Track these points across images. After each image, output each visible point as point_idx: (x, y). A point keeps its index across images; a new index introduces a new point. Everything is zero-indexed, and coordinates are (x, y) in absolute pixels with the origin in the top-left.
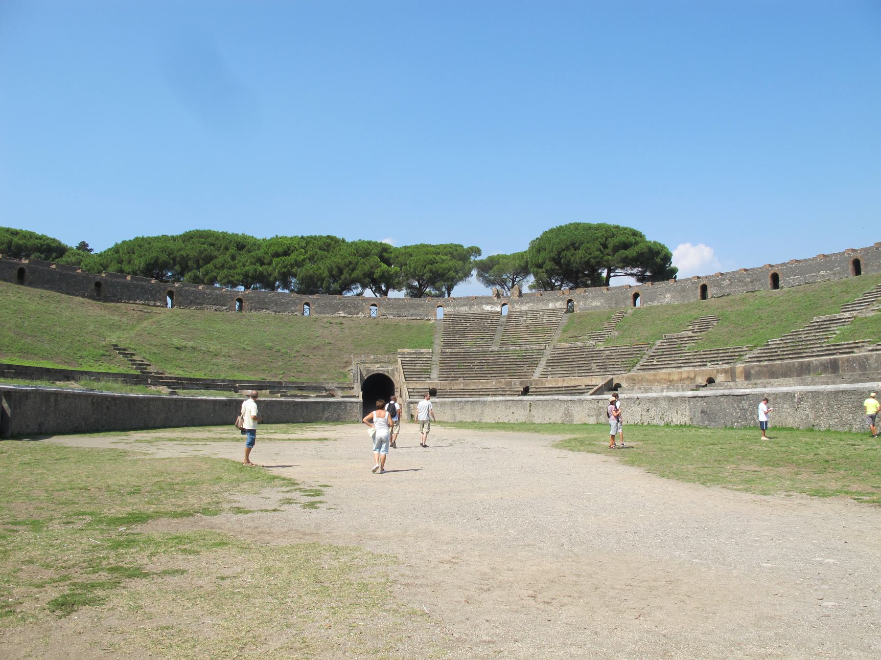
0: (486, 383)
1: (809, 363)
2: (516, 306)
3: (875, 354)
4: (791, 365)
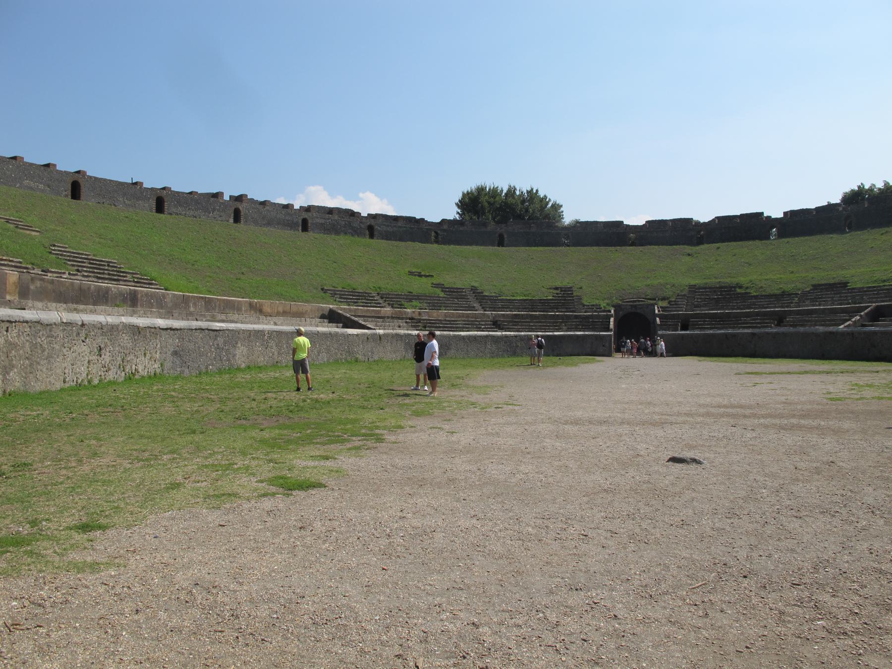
3: (171, 294)
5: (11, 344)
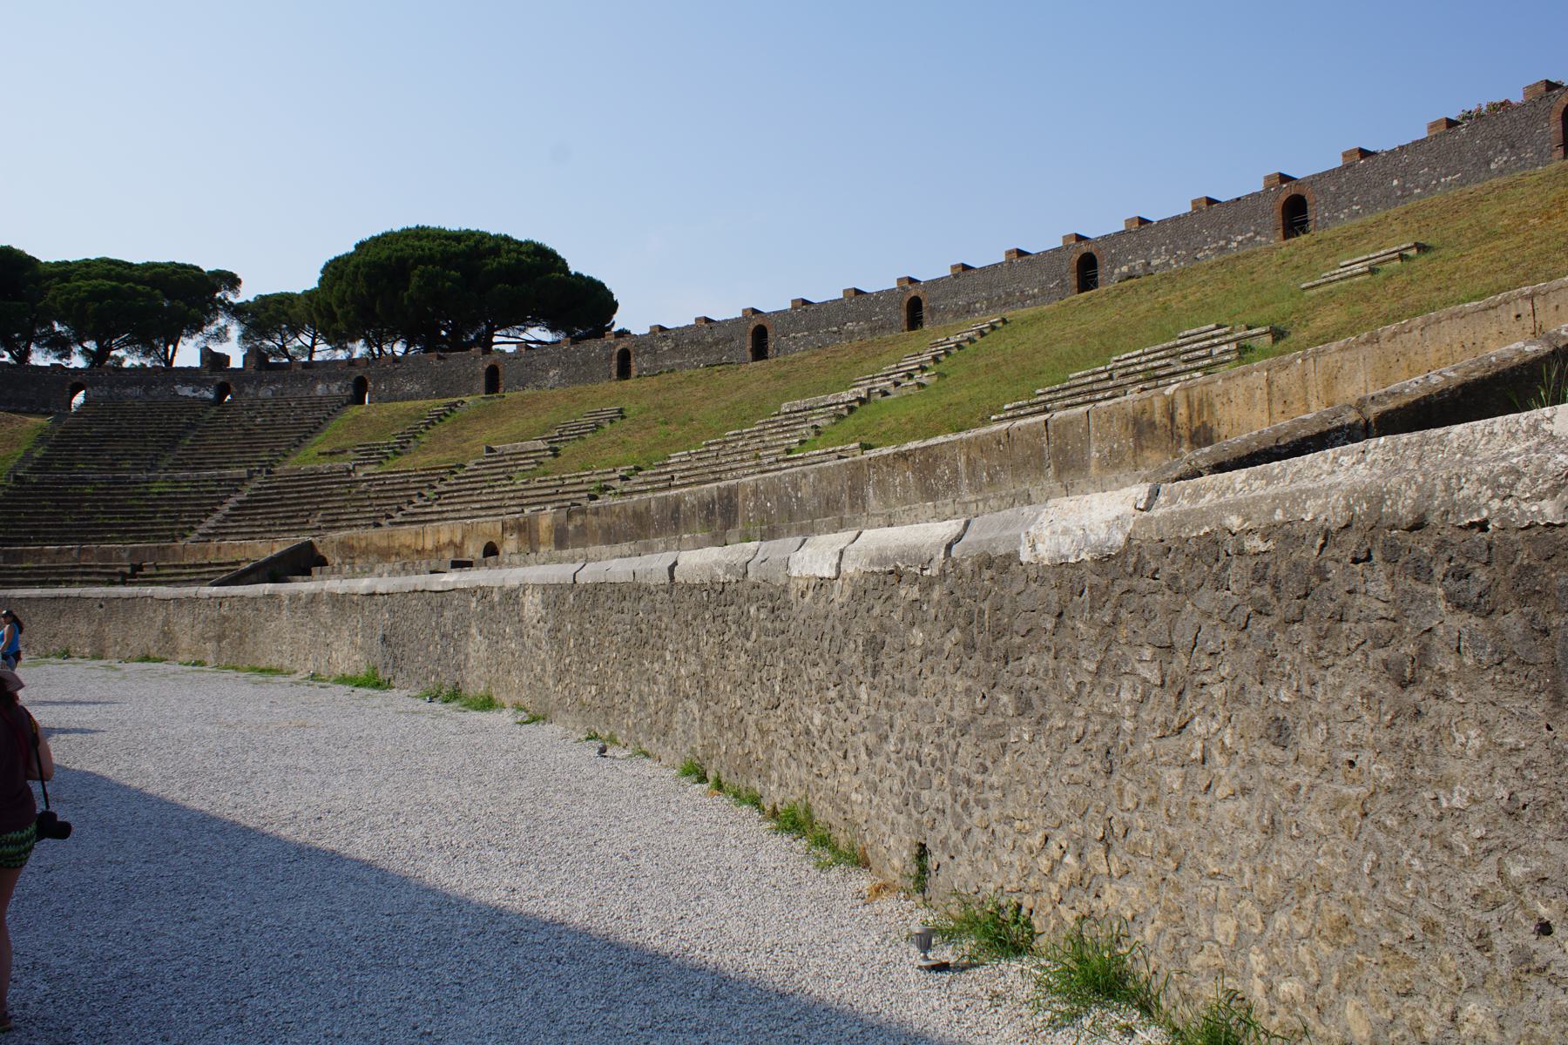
0: (59, 552)
1: (678, 500)
2: (247, 390)
4: (642, 508)
5: (224, 617)
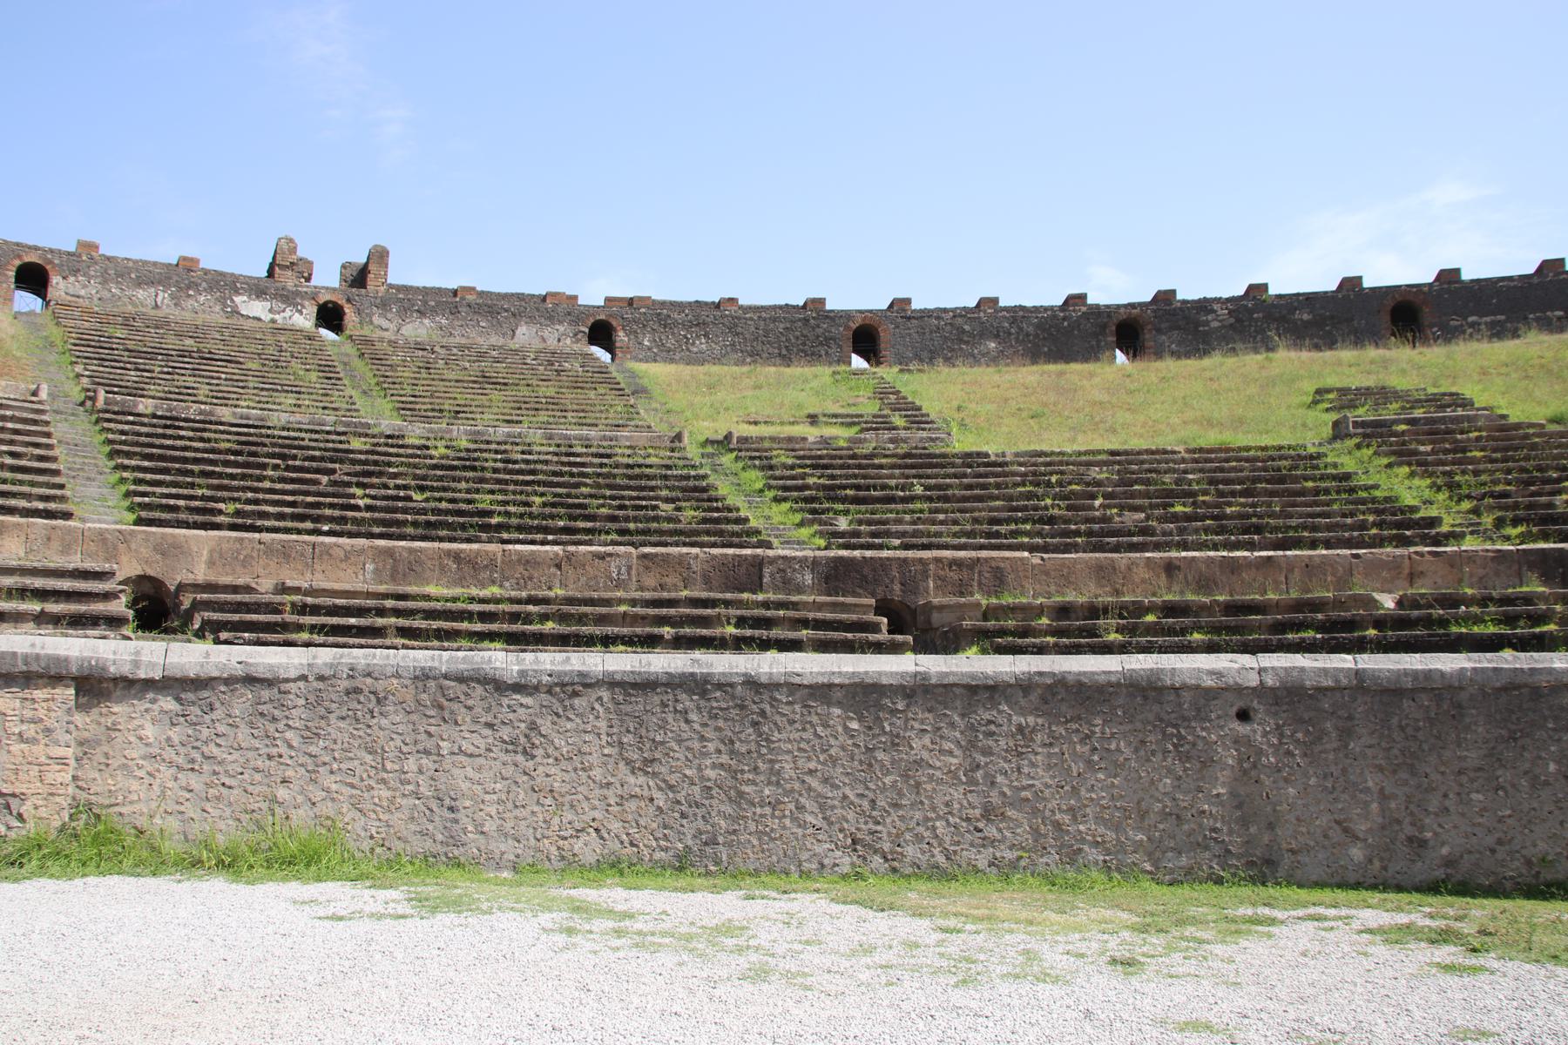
2: (377, 320)
